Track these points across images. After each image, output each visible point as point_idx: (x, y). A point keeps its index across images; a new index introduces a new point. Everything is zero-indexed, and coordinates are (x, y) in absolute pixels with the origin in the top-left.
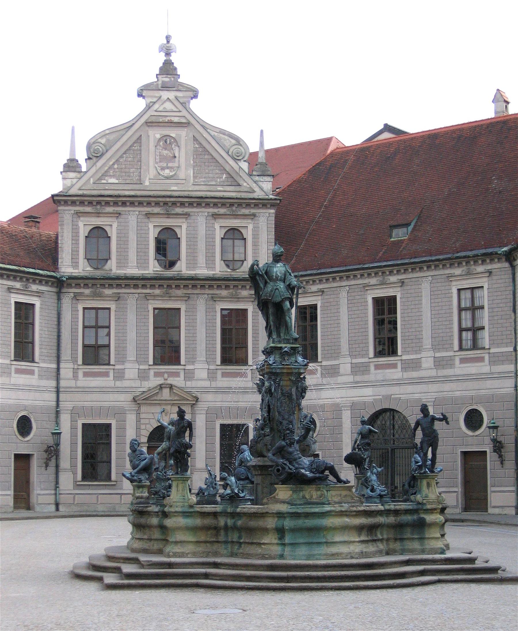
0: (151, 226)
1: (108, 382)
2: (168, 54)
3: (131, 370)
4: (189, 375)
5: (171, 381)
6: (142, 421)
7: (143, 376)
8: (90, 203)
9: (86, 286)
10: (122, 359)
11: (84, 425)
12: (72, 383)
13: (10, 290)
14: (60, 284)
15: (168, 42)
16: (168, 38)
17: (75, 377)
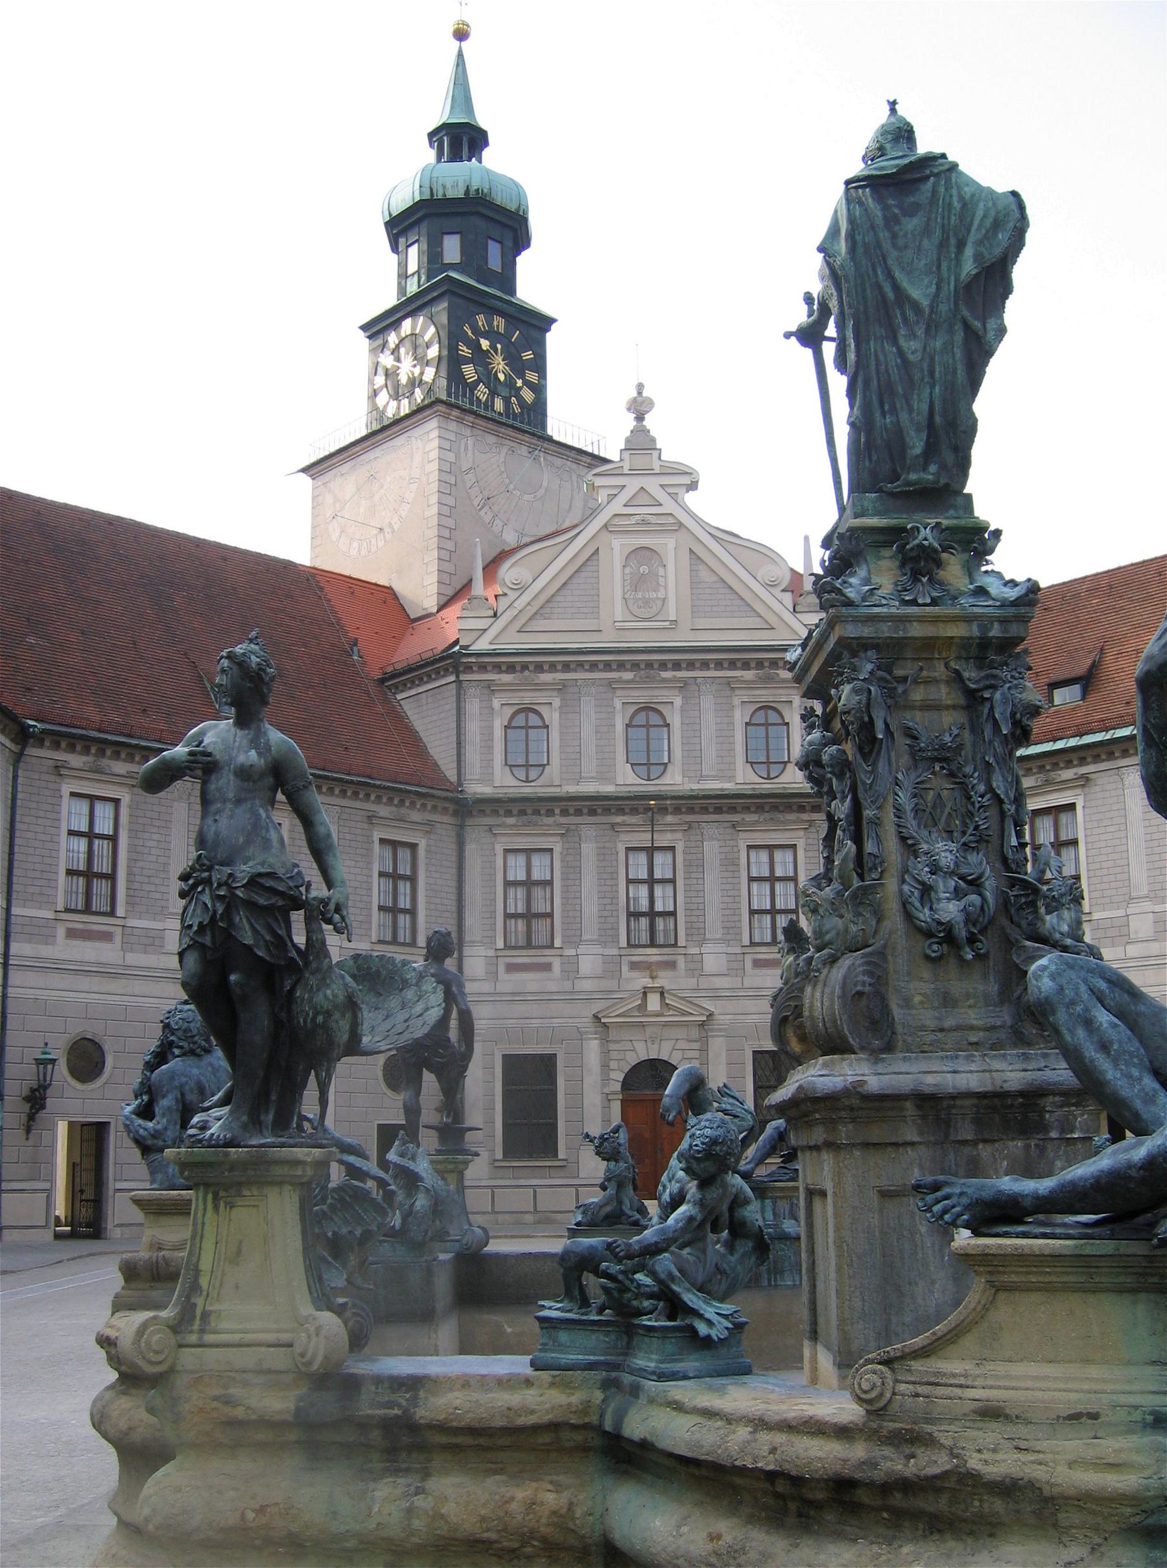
0: (618, 704)
1: (552, 982)
2: (640, 418)
3: (589, 962)
4: (696, 968)
5: (664, 980)
6: (614, 1055)
7: (611, 969)
8: (511, 668)
9: (509, 813)
10: (575, 939)
11: (507, 1058)
12: (487, 987)
13: (371, 818)
14: (464, 809)
15: (640, 393)
16: (640, 387)
17: (493, 976)
